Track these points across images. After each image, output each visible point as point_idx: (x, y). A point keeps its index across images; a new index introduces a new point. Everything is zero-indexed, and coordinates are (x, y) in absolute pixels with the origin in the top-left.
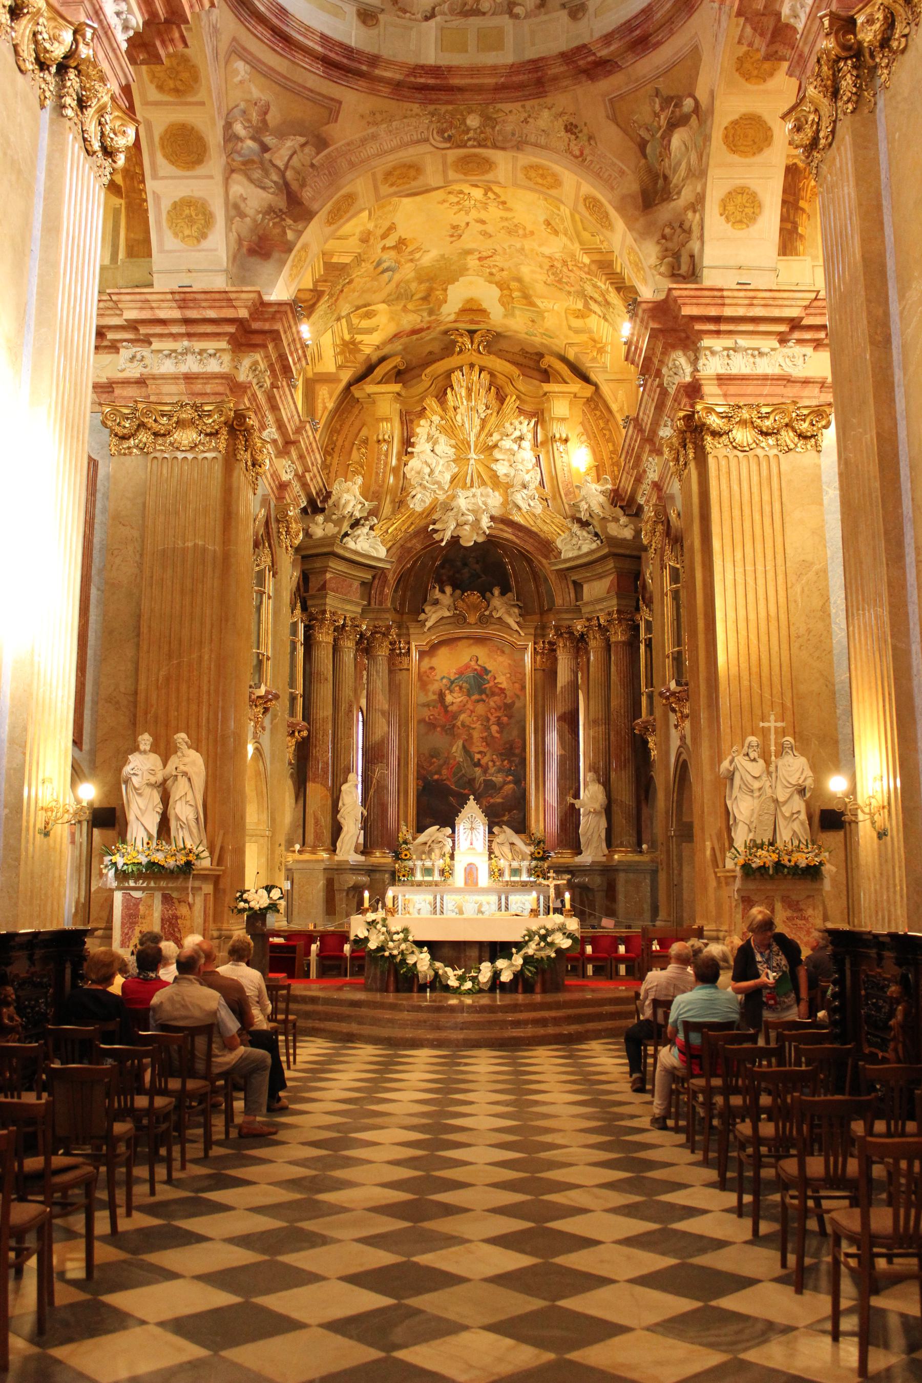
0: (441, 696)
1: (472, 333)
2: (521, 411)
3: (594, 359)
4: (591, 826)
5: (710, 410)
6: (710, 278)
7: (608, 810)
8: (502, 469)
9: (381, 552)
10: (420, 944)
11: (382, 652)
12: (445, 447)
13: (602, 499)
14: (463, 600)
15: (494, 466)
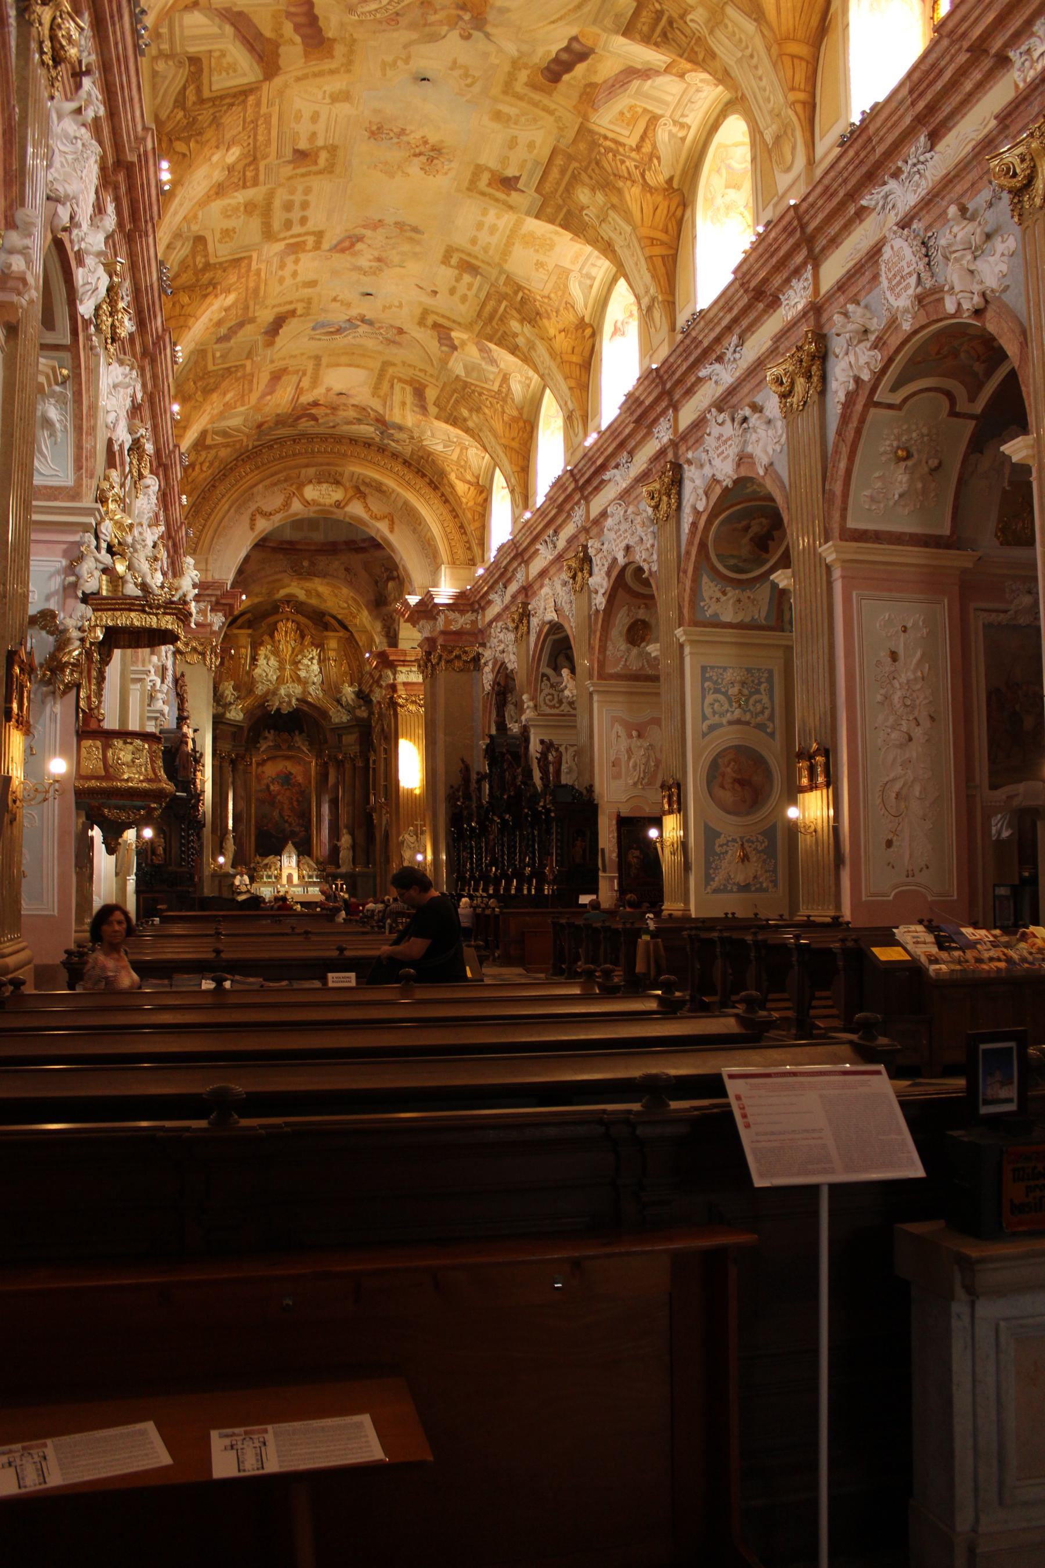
0: (268, 787)
1: (288, 602)
2: (313, 644)
4: (345, 854)
5: (400, 697)
6: (403, 645)
7: (354, 847)
8: (303, 674)
9: (240, 717)
10: (297, 903)
11: (241, 767)
12: (273, 662)
13: (353, 696)
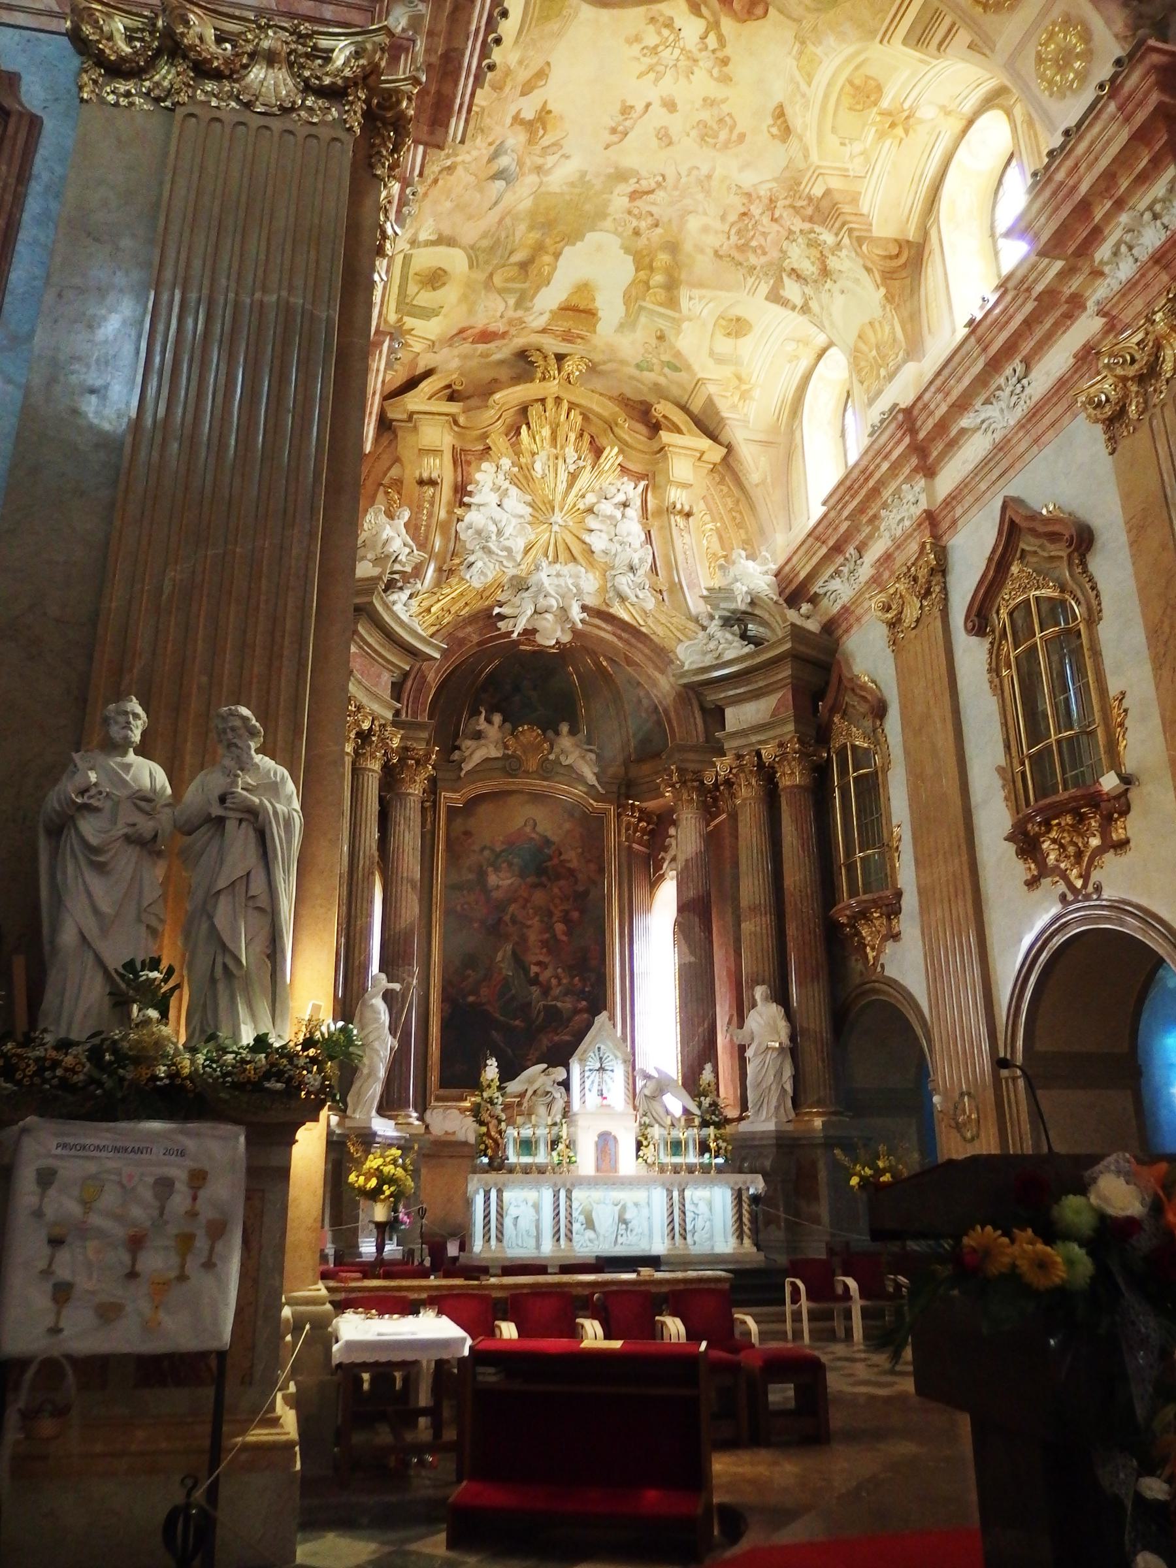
0: (482, 875)
1: (560, 358)
2: (624, 470)
3: (734, 407)
8: (598, 542)
12: (516, 502)
14: (516, 737)
15: (587, 538)
